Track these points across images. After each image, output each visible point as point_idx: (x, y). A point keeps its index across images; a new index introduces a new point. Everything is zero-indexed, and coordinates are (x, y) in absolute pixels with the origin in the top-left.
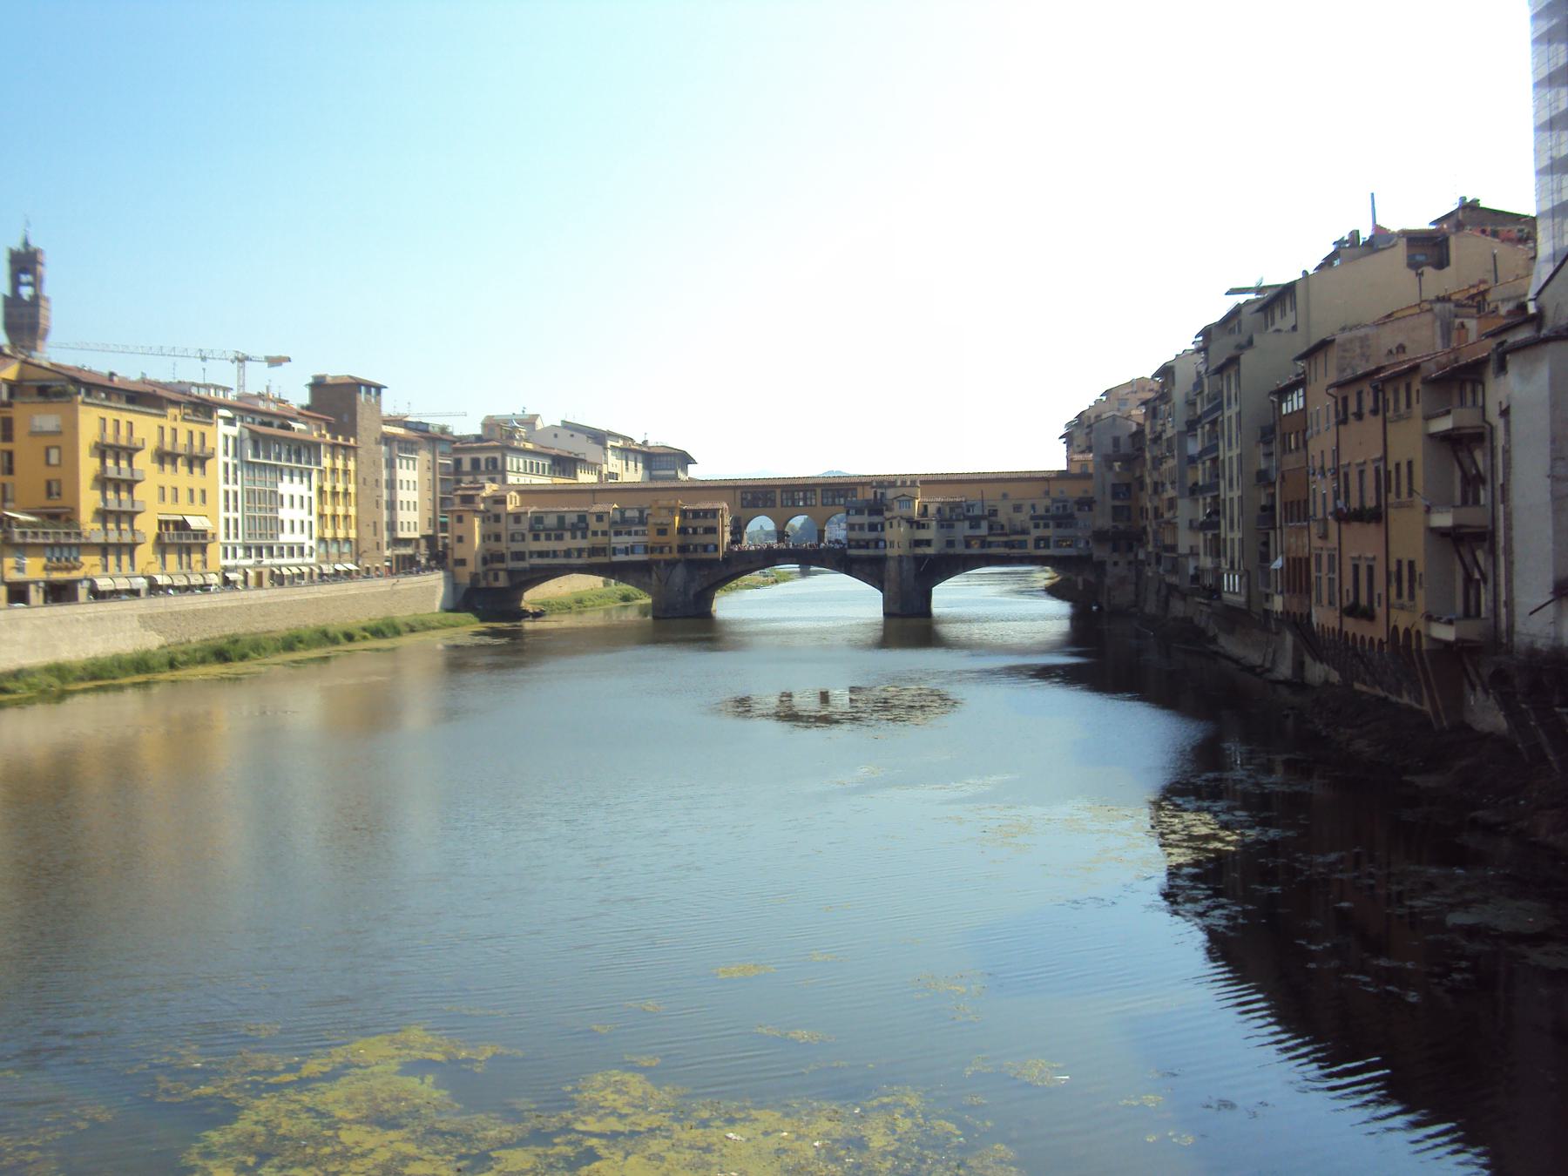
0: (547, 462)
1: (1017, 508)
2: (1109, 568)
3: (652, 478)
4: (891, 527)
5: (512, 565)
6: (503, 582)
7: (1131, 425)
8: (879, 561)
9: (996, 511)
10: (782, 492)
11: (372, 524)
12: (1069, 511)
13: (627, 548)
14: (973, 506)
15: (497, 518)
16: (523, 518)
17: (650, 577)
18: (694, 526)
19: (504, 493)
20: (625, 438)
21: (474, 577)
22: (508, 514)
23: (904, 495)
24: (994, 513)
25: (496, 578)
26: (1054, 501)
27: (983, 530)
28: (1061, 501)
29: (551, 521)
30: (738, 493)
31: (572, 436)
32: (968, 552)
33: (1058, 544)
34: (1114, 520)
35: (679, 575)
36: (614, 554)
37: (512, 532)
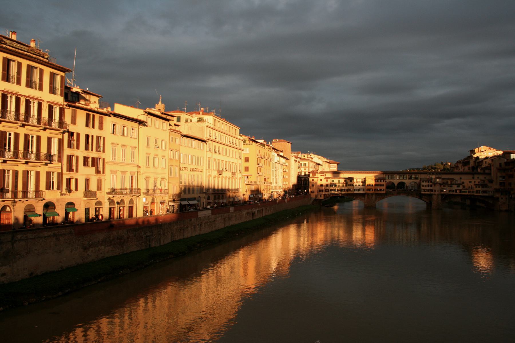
0: (315, 164)
1: (470, 182)
2: (500, 199)
4: (435, 186)
6: (322, 198)
8: (430, 195)
9: (464, 182)
12: (485, 183)
13: (358, 189)
14: (457, 181)
17: (364, 197)
21: (316, 196)
23: (439, 177)
24: (463, 183)
25: (321, 196)
26: (481, 180)
27: (461, 187)
28: (483, 180)
32: (456, 193)
33: (484, 192)
35: (374, 196)
36: (355, 191)
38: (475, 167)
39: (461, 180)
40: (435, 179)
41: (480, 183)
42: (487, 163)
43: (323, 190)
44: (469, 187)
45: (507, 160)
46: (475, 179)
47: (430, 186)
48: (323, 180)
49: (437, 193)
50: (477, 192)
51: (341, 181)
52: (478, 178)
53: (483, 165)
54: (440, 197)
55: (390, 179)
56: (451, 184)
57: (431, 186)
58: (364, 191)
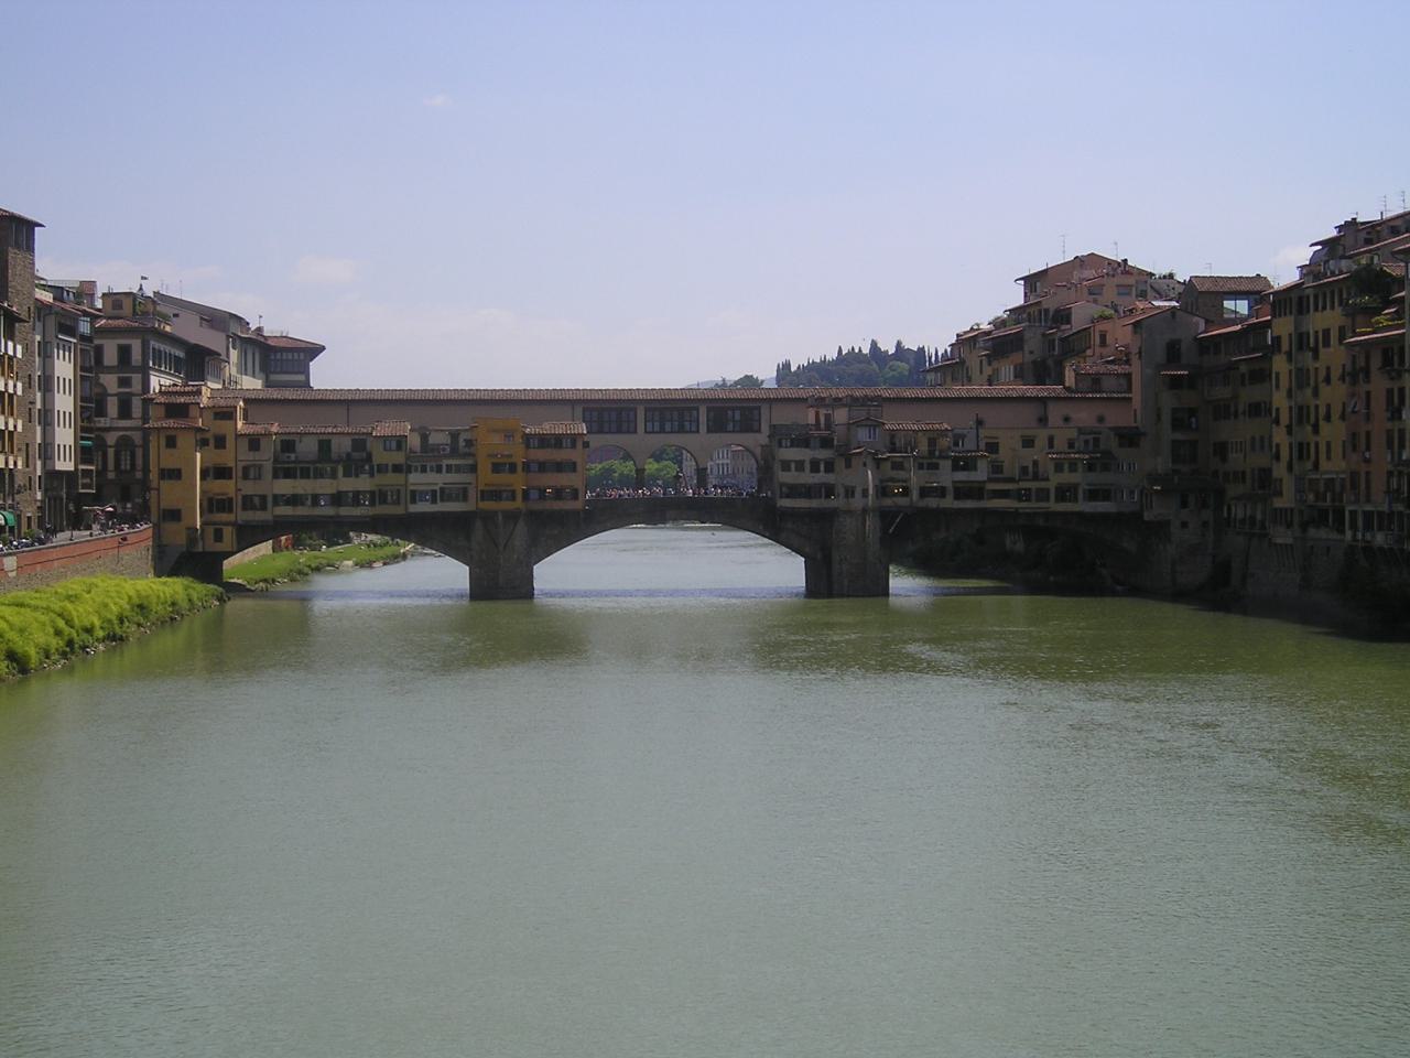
1: (1028, 443)
3: (268, 384)
4: (848, 465)
5: (244, 516)
7: (1197, 324)
8: (825, 518)
10: (646, 410)
11: (24, 448)
12: (1102, 447)
13: (434, 492)
14: (963, 437)
15: (220, 442)
16: (263, 443)
18: (541, 459)
19: (231, 402)
20: (239, 319)
22: (238, 436)
24: (993, 447)
25: (219, 537)
26: (1081, 431)
29: (307, 448)
30: (579, 411)
31: (176, 315)
33: (1093, 495)
34: (1174, 462)
35: (521, 529)
36: (413, 501)
37: (243, 464)
38: (1050, 362)
39: (982, 433)
40: (849, 429)
41: (1076, 445)
42: (1109, 340)
43: (231, 499)
44: (1024, 470)
45: (1207, 322)
46: (1050, 424)
47: (822, 467)
48: (230, 442)
49: (857, 503)
50: (1065, 493)
51: (334, 447)
52: (1067, 419)
53: (1089, 352)
54: (871, 524)
55: (610, 432)
56: (931, 453)
57: (830, 467)
58: (465, 498)
